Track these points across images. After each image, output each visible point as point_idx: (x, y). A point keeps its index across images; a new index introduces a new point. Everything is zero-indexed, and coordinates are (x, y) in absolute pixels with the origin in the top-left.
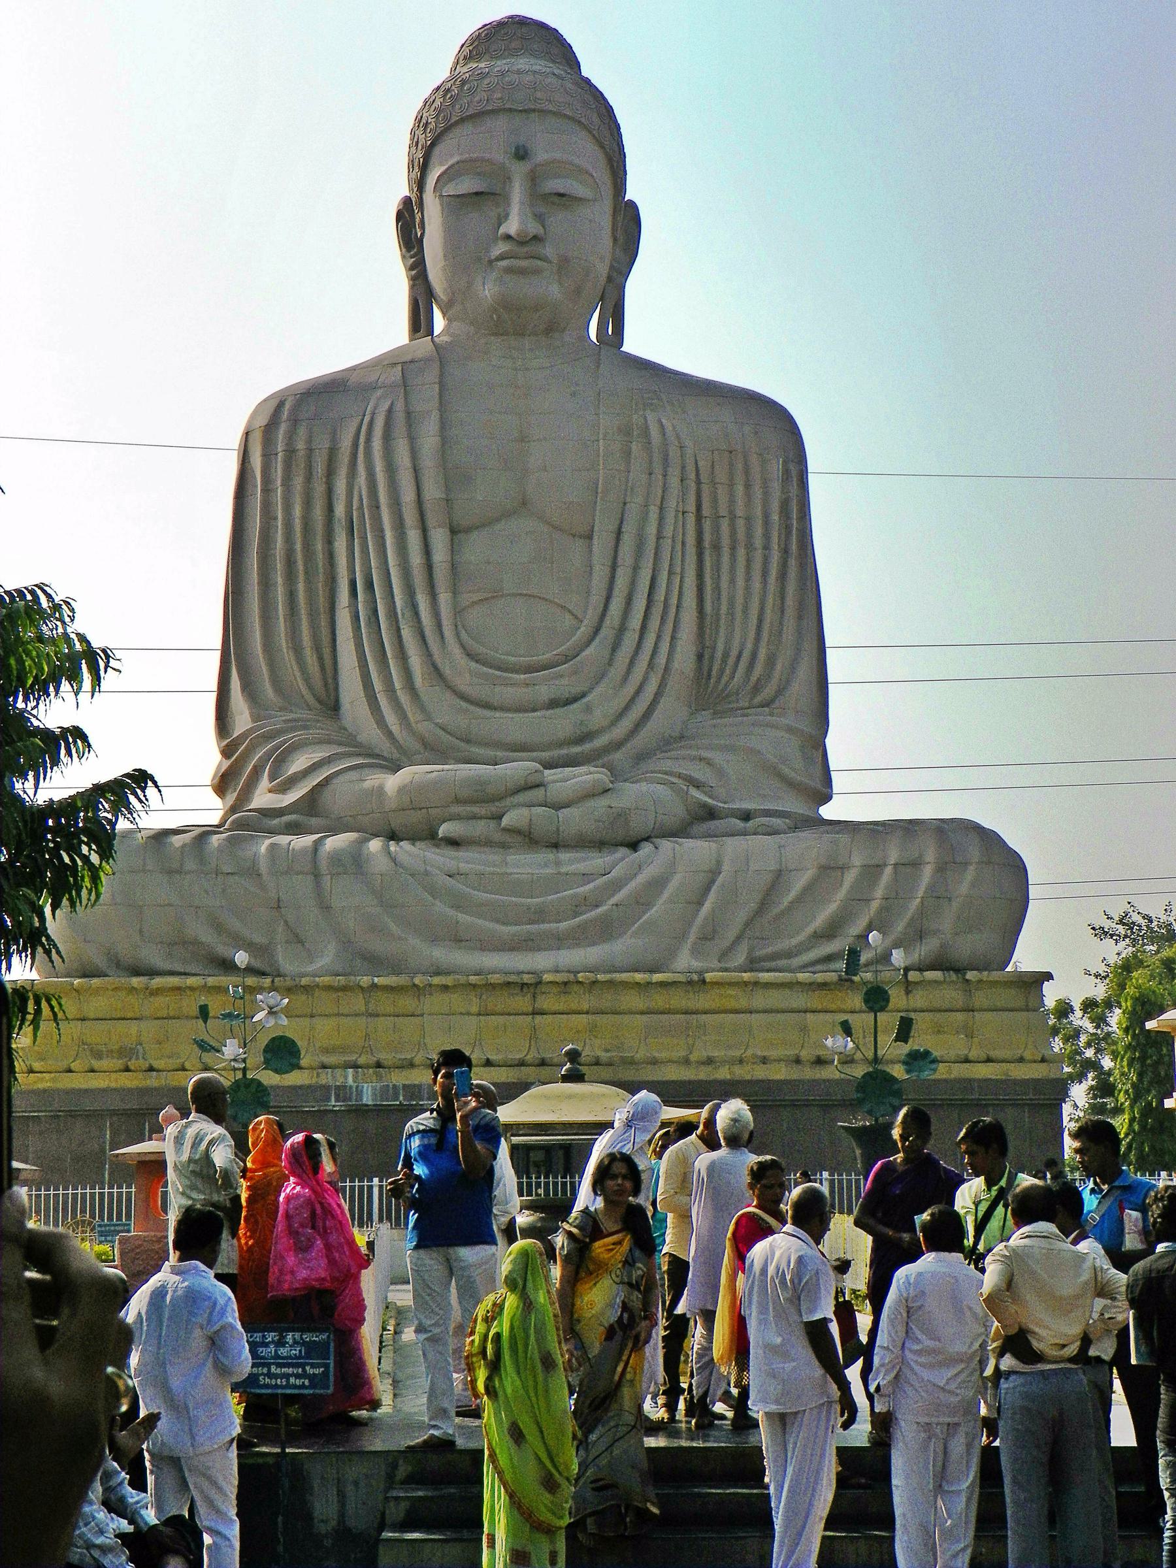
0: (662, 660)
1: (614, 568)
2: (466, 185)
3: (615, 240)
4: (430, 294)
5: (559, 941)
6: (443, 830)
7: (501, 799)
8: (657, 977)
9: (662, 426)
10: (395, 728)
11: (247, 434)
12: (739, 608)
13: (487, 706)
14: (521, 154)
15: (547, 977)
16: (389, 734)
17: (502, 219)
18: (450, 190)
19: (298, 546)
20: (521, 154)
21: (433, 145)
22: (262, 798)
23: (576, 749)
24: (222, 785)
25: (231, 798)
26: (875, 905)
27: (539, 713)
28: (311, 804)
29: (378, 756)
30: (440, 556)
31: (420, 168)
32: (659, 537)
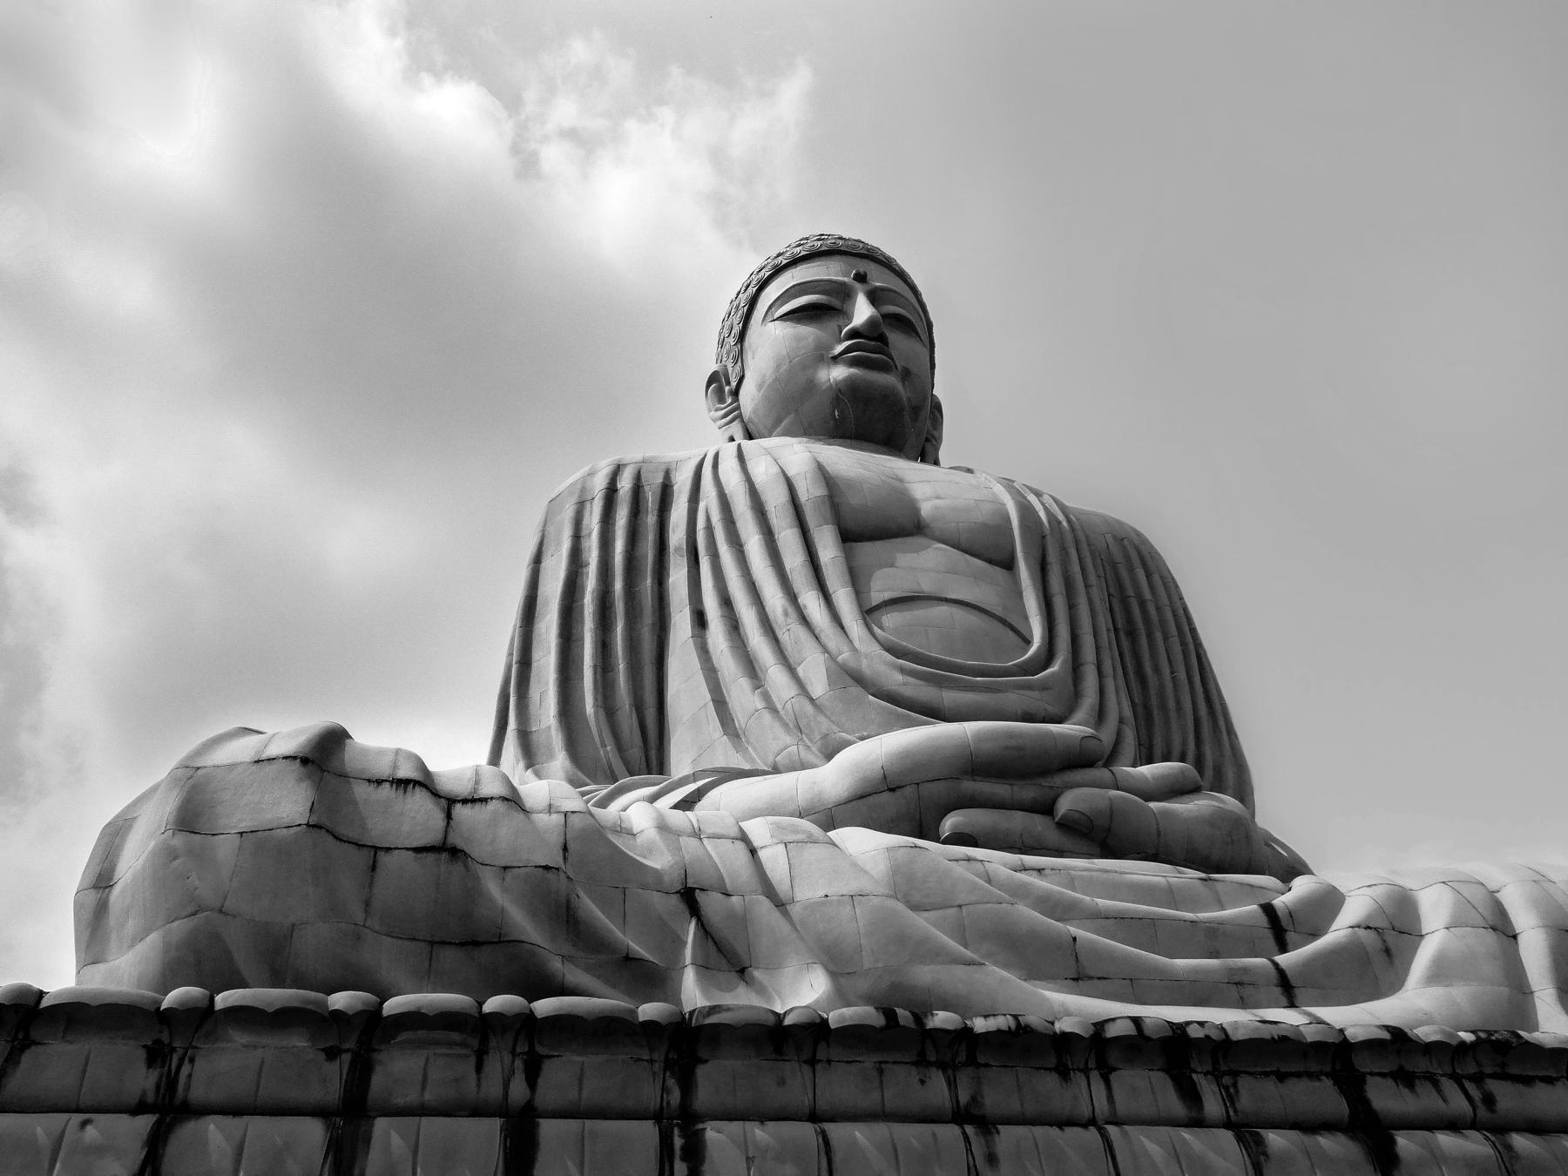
7: (1045, 772)
12: (1171, 704)
14: (861, 278)
17: (850, 319)
19: (618, 585)
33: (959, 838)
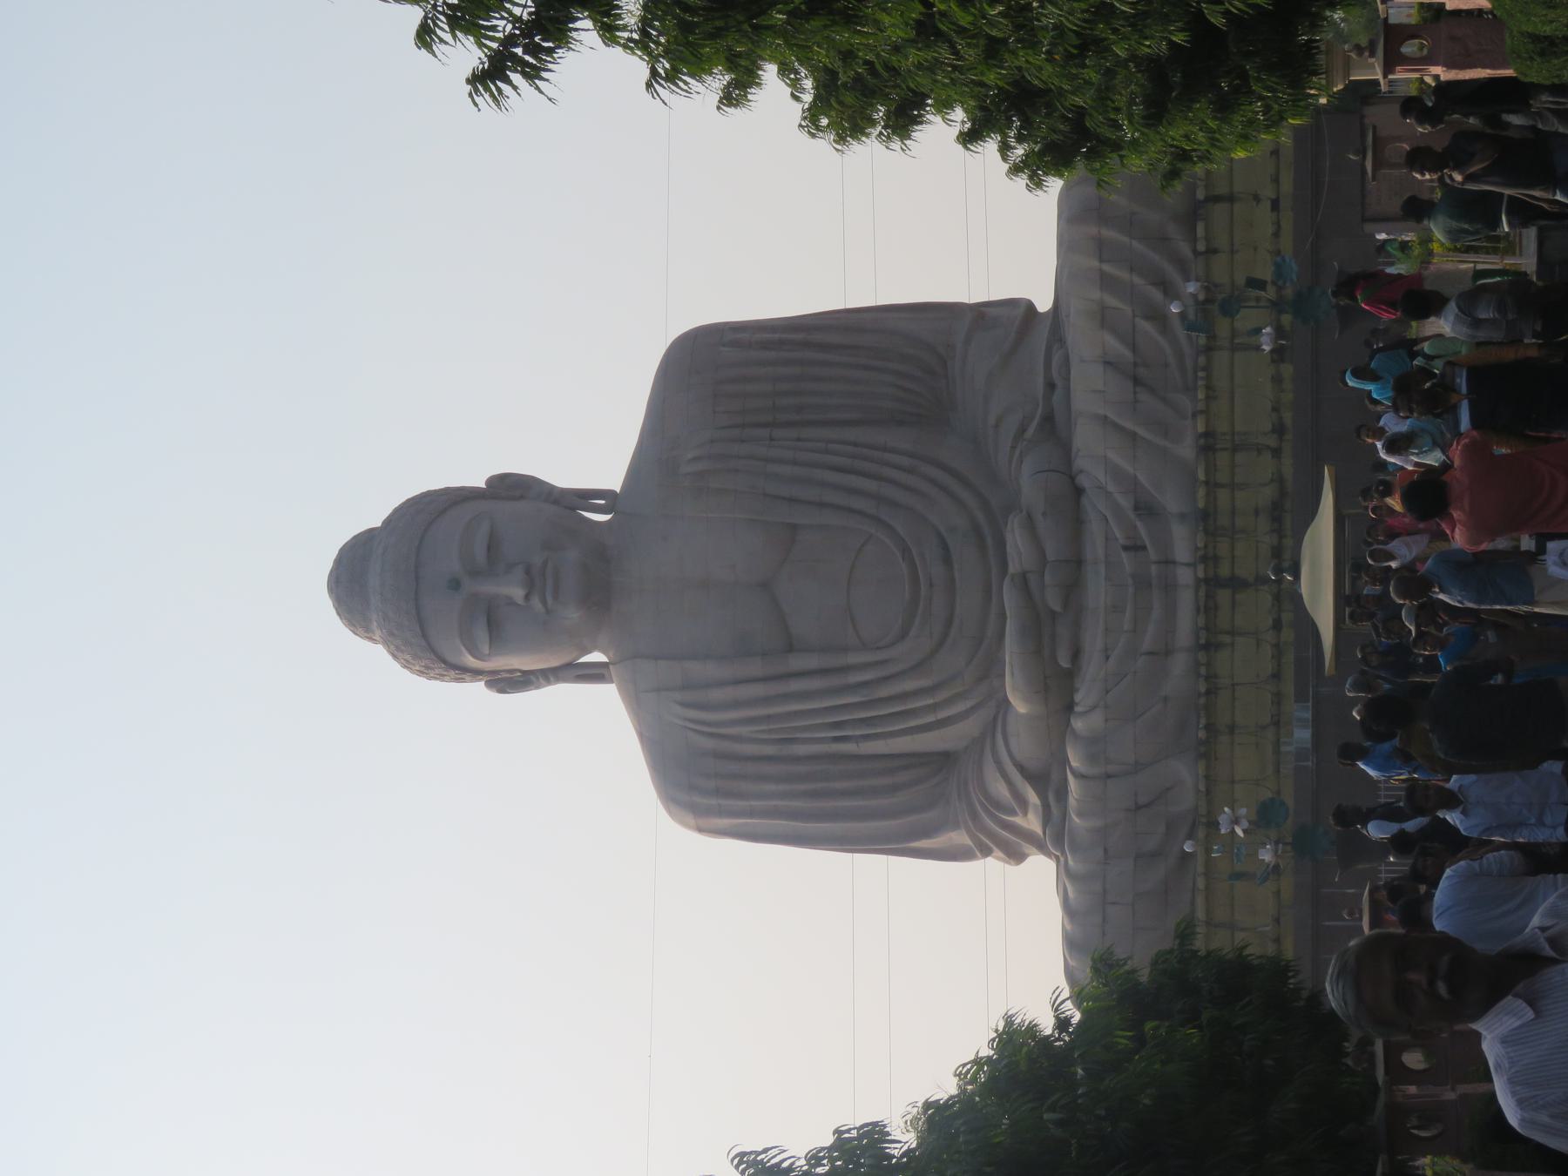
0: (905, 461)
1: (822, 505)
2: (482, 634)
3: (521, 497)
4: (570, 666)
5: (1168, 562)
8: (1201, 476)
9: (696, 459)
10: (968, 704)
11: (700, 830)
13: (949, 622)
15: (1201, 574)
16: (974, 709)
17: (511, 602)
18: (486, 649)
19: (802, 787)
20: (455, 585)
21: (444, 662)
22: (1032, 822)
23: (989, 541)
24: (1016, 856)
25: (1027, 848)
26: (1137, 280)
27: (957, 575)
28: (1038, 779)
29: (995, 719)
30: (812, 662)
31: (462, 672)
32: (795, 463)
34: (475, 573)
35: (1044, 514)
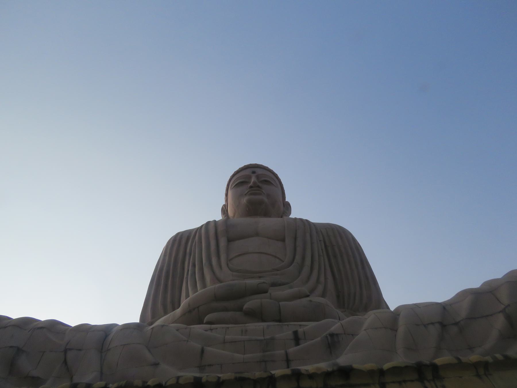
3: (284, 206)
6: (207, 318)
14: (254, 172)
32: (312, 243)
33: (210, 323)
34: (258, 177)
35: (311, 301)
